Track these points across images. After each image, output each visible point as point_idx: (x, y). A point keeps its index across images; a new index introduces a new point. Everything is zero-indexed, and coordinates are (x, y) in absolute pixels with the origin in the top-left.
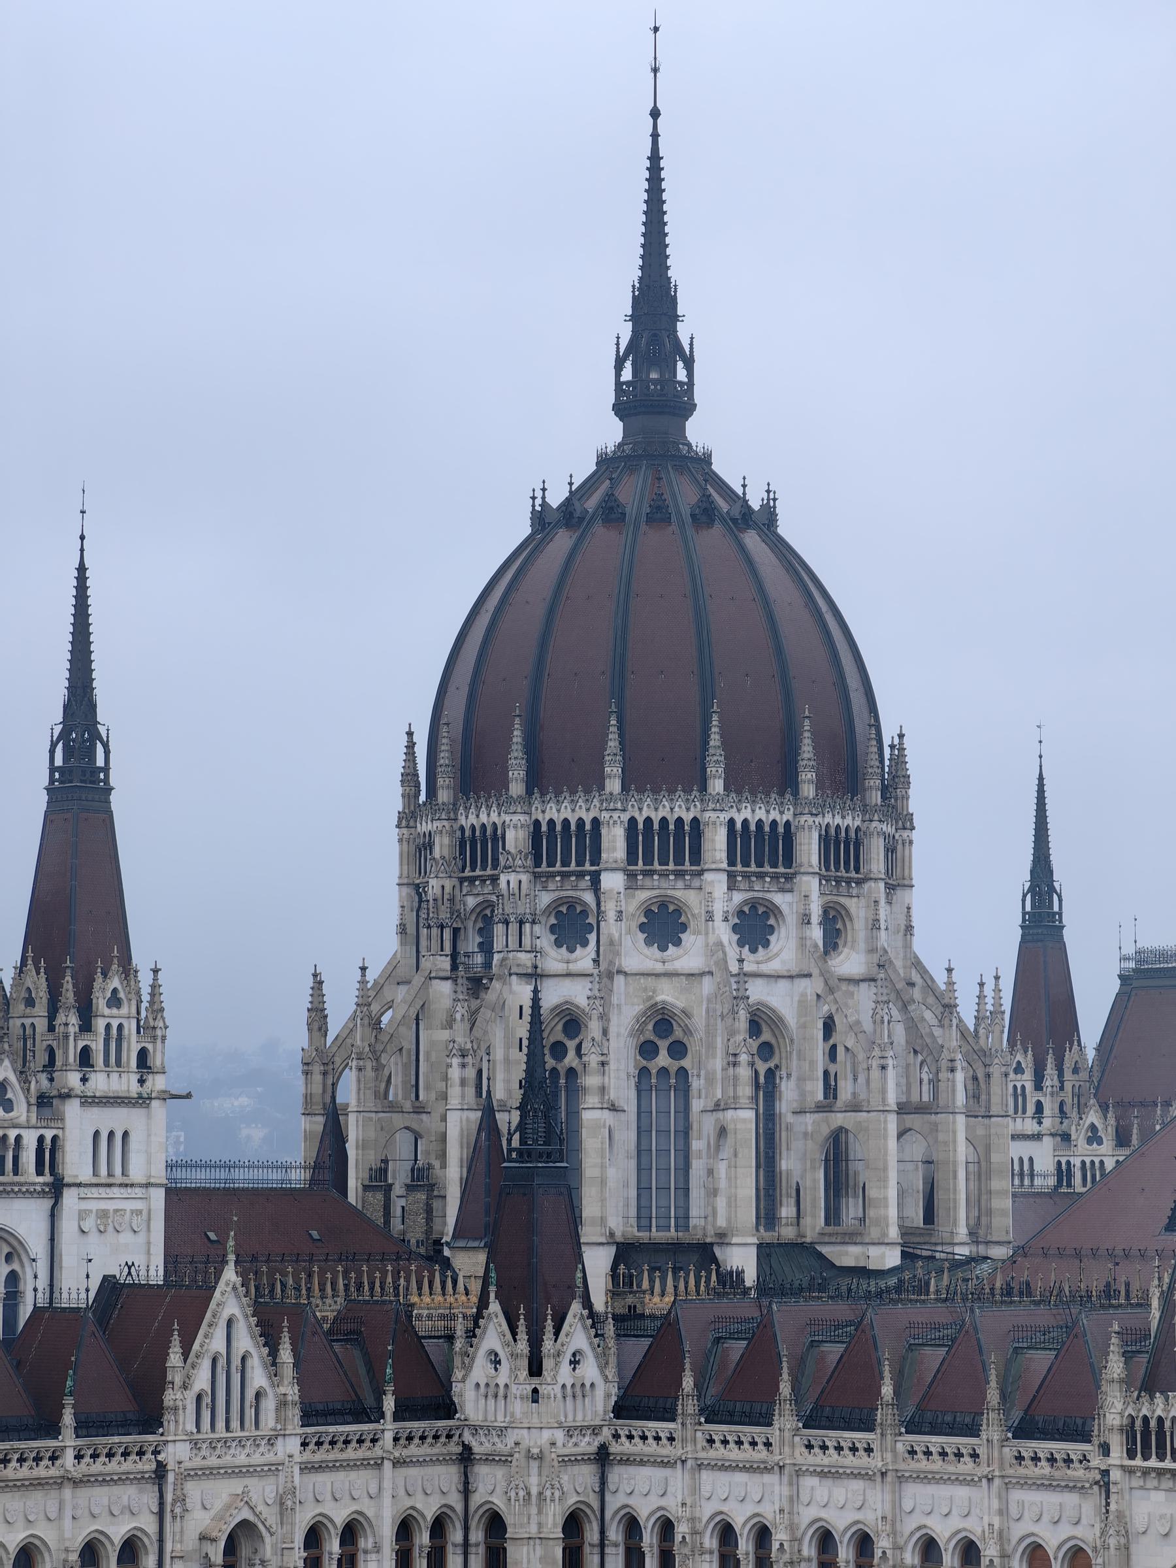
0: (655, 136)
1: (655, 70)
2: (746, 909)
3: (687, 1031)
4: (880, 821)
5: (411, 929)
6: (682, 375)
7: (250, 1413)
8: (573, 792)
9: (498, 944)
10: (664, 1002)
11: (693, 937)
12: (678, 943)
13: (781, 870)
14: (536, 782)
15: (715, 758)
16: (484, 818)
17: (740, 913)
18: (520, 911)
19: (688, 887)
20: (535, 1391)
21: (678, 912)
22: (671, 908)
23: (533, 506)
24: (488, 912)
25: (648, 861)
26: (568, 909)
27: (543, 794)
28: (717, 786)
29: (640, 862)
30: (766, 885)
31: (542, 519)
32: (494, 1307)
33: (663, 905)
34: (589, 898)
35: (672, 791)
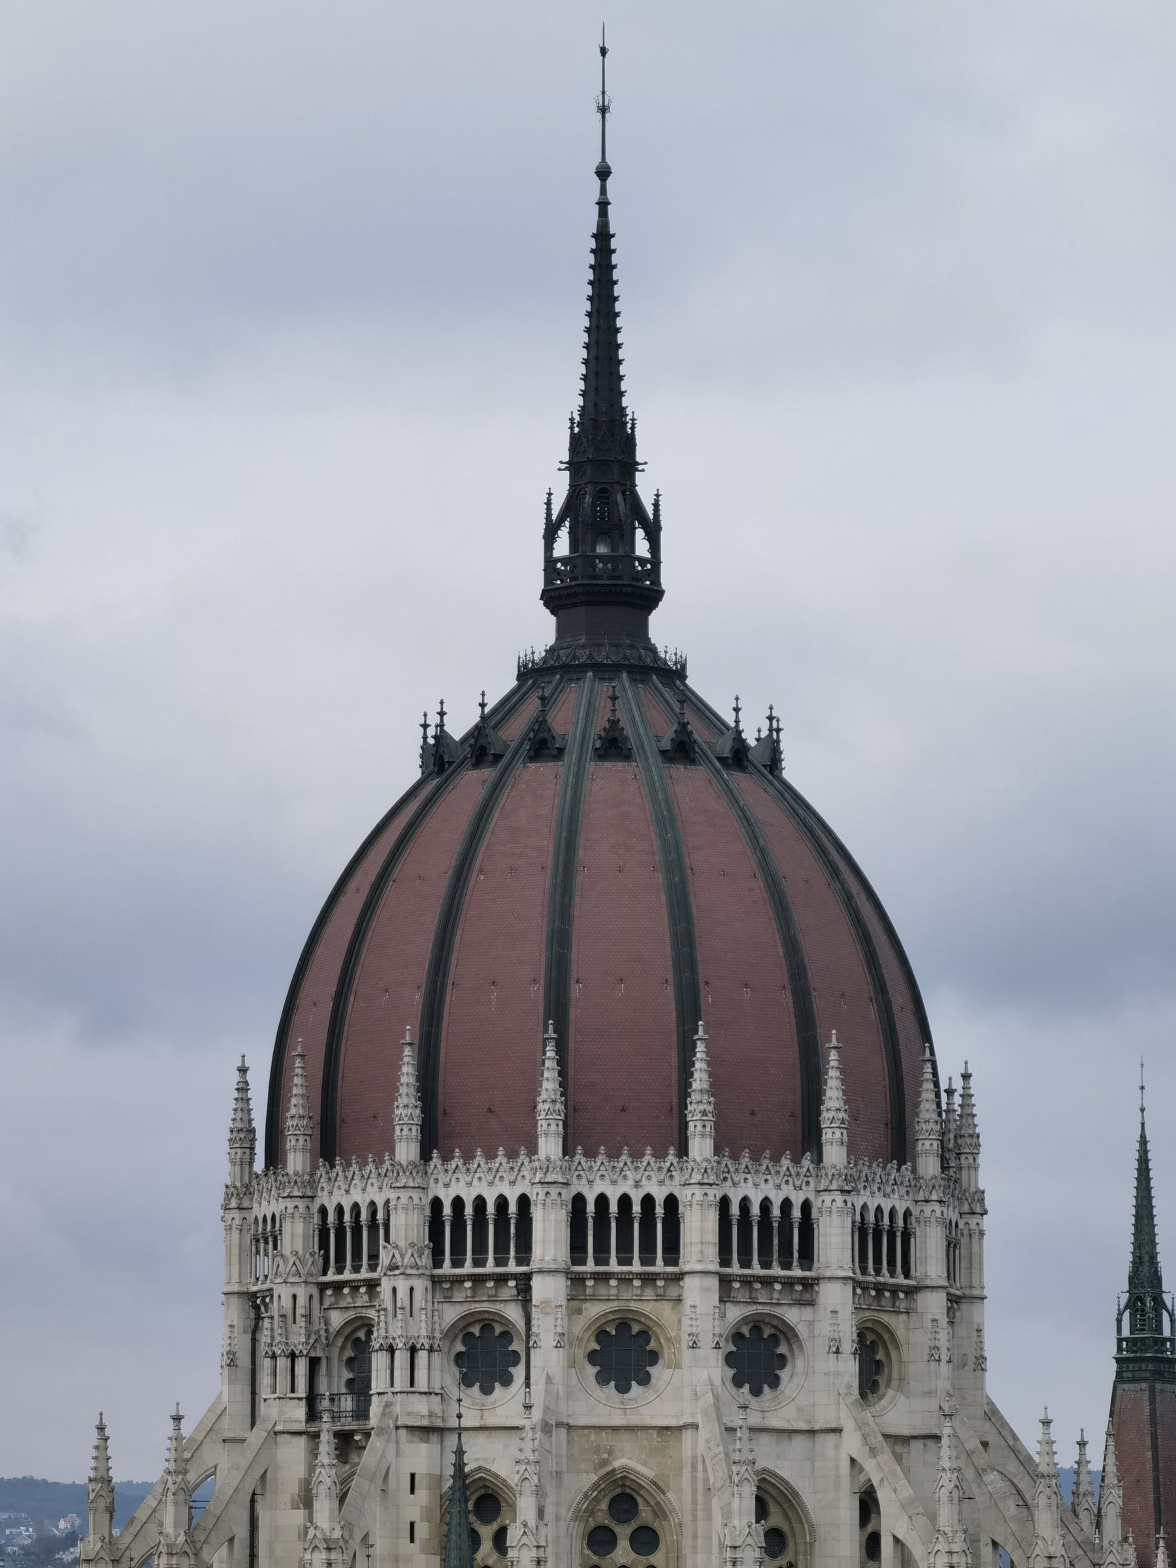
0: (603, 205)
1: (603, 110)
2: (745, 1331)
3: (659, 1512)
4: (940, 1202)
5: (244, 1360)
6: (642, 548)
8: (490, 1156)
9: (378, 1381)
10: (624, 1469)
11: (669, 1372)
12: (645, 1380)
13: (797, 1272)
14: (433, 1140)
15: (701, 1107)
16: (357, 1196)
17: (737, 1337)
18: (413, 1332)
19: (660, 1298)
21: (645, 1335)
22: (636, 1329)
23: (425, 738)
25: (601, 1259)
26: (482, 1330)
27: (446, 1158)
28: (701, 1147)
30: (776, 1295)
31: (440, 757)
33: (623, 1325)
34: (513, 1313)
35: (636, 1155)
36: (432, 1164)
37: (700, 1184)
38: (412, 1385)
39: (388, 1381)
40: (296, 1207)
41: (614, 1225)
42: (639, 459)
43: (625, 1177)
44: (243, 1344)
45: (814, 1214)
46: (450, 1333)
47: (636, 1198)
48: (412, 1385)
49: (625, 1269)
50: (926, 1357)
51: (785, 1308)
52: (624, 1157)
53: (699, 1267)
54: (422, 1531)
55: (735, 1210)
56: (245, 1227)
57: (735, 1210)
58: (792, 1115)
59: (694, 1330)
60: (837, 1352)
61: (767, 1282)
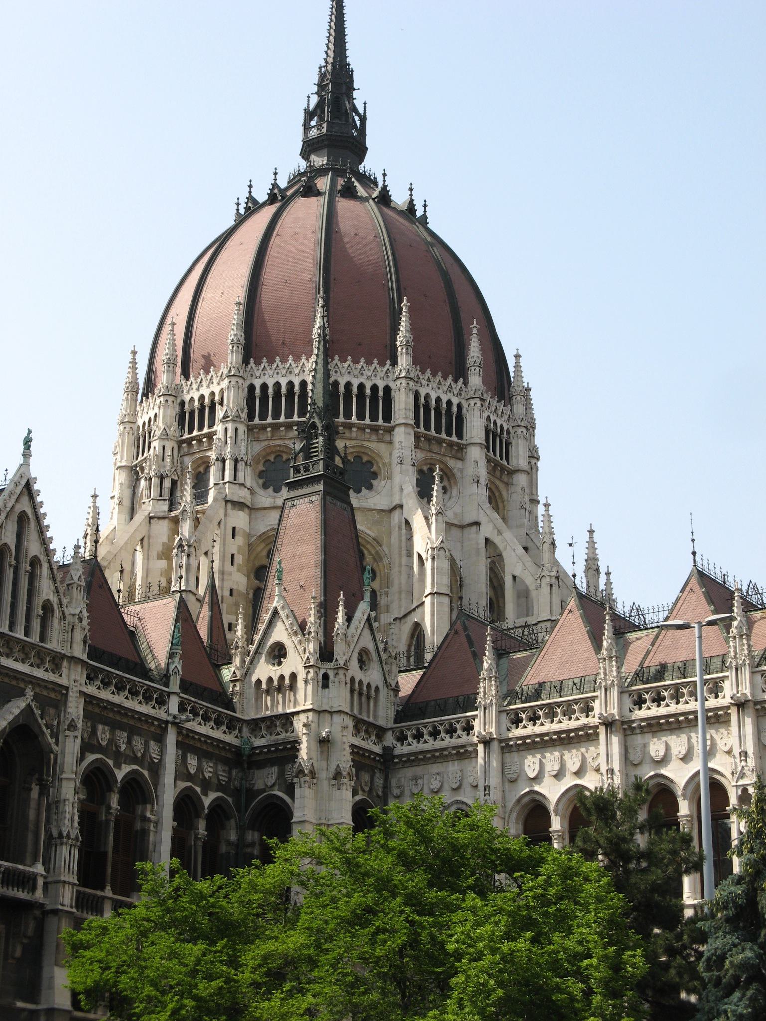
3: (378, 558)
4: (526, 427)
5: (127, 502)
7: (36, 624)
11: (383, 483)
12: (370, 487)
19: (380, 441)
20: (325, 677)
21: (370, 463)
22: (365, 459)
23: (238, 210)
24: (202, 469)
26: (275, 458)
28: (404, 361)
29: (341, 416)
30: (443, 450)
35: (369, 363)
41: (354, 399)
42: (355, 86)
44: (128, 493)
45: (464, 411)
46: (256, 460)
47: (368, 385)
48: (235, 479)
50: (519, 507)
51: (448, 458)
53: (403, 421)
54: (239, 559)
55: (422, 400)
57: (422, 400)
58: (450, 363)
60: (478, 482)
61: (440, 442)
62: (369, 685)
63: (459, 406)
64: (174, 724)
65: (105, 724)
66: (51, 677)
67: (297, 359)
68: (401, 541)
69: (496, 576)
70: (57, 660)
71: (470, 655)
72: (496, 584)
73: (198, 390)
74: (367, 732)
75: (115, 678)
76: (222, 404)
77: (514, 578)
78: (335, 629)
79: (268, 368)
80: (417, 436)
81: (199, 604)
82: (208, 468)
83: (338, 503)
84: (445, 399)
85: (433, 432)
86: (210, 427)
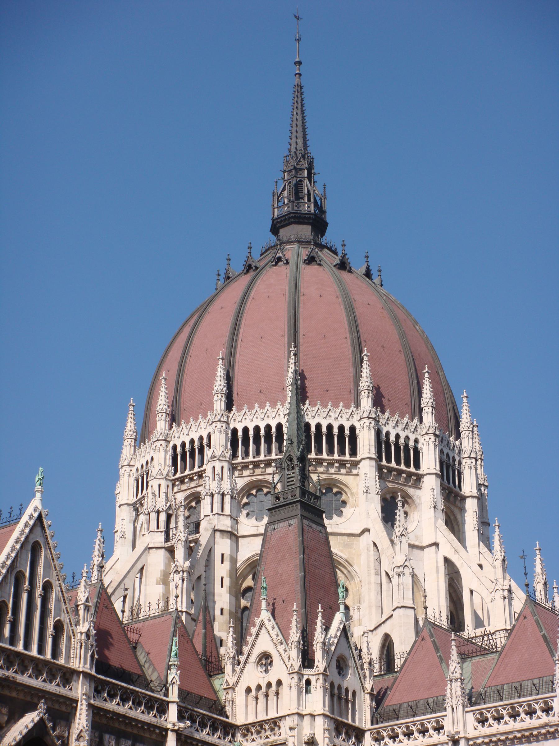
2: (388, 497)
8: (262, 407)
11: (353, 509)
12: (340, 514)
19: (349, 473)
20: (308, 682)
26: (257, 492)
32: (265, 615)
35: (336, 405)
36: (232, 412)
37: (368, 418)
38: (222, 511)
39: (210, 510)
40: (161, 445)
43: (330, 416)
45: (420, 446)
48: (222, 511)
49: (331, 458)
52: (329, 407)
56: (131, 474)
59: (366, 484)
61: (400, 472)
62: (347, 690)
63: (416, 441)
64: (173, 730)
65: (111, 733)
66: (63, 691)
67: (273, 405)
68: (369, 561)
69: (455, 591)
70: (68, 676)
71: (437, 660)
72: (455, 599)
73: (188, 435)
74: (347, 734)
75: (120, 689)
76: (209, 445)
77: (471, 592)
78: (315, 638)
79: (248, 414)
80: (380, 468)
81: (194, 623)
82: (198, 502)
83: (314, 526)
84: (403, 435)
85: (393, 464)
86: (199, 467)
